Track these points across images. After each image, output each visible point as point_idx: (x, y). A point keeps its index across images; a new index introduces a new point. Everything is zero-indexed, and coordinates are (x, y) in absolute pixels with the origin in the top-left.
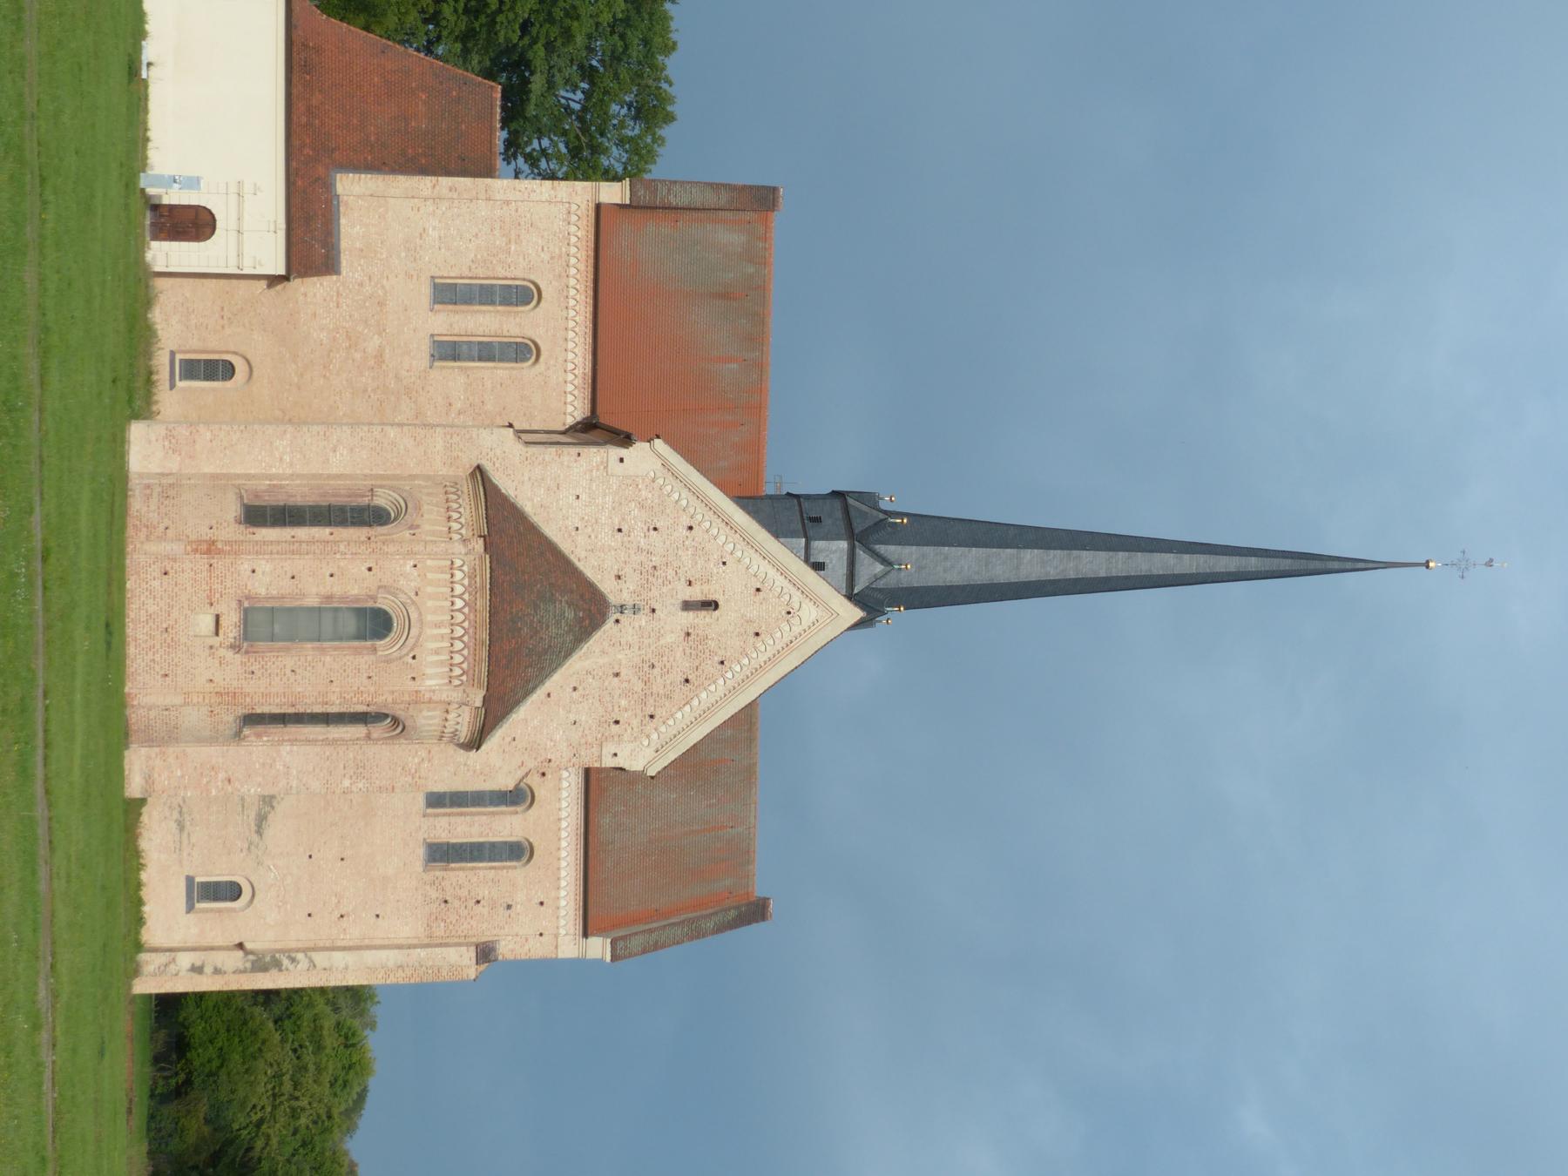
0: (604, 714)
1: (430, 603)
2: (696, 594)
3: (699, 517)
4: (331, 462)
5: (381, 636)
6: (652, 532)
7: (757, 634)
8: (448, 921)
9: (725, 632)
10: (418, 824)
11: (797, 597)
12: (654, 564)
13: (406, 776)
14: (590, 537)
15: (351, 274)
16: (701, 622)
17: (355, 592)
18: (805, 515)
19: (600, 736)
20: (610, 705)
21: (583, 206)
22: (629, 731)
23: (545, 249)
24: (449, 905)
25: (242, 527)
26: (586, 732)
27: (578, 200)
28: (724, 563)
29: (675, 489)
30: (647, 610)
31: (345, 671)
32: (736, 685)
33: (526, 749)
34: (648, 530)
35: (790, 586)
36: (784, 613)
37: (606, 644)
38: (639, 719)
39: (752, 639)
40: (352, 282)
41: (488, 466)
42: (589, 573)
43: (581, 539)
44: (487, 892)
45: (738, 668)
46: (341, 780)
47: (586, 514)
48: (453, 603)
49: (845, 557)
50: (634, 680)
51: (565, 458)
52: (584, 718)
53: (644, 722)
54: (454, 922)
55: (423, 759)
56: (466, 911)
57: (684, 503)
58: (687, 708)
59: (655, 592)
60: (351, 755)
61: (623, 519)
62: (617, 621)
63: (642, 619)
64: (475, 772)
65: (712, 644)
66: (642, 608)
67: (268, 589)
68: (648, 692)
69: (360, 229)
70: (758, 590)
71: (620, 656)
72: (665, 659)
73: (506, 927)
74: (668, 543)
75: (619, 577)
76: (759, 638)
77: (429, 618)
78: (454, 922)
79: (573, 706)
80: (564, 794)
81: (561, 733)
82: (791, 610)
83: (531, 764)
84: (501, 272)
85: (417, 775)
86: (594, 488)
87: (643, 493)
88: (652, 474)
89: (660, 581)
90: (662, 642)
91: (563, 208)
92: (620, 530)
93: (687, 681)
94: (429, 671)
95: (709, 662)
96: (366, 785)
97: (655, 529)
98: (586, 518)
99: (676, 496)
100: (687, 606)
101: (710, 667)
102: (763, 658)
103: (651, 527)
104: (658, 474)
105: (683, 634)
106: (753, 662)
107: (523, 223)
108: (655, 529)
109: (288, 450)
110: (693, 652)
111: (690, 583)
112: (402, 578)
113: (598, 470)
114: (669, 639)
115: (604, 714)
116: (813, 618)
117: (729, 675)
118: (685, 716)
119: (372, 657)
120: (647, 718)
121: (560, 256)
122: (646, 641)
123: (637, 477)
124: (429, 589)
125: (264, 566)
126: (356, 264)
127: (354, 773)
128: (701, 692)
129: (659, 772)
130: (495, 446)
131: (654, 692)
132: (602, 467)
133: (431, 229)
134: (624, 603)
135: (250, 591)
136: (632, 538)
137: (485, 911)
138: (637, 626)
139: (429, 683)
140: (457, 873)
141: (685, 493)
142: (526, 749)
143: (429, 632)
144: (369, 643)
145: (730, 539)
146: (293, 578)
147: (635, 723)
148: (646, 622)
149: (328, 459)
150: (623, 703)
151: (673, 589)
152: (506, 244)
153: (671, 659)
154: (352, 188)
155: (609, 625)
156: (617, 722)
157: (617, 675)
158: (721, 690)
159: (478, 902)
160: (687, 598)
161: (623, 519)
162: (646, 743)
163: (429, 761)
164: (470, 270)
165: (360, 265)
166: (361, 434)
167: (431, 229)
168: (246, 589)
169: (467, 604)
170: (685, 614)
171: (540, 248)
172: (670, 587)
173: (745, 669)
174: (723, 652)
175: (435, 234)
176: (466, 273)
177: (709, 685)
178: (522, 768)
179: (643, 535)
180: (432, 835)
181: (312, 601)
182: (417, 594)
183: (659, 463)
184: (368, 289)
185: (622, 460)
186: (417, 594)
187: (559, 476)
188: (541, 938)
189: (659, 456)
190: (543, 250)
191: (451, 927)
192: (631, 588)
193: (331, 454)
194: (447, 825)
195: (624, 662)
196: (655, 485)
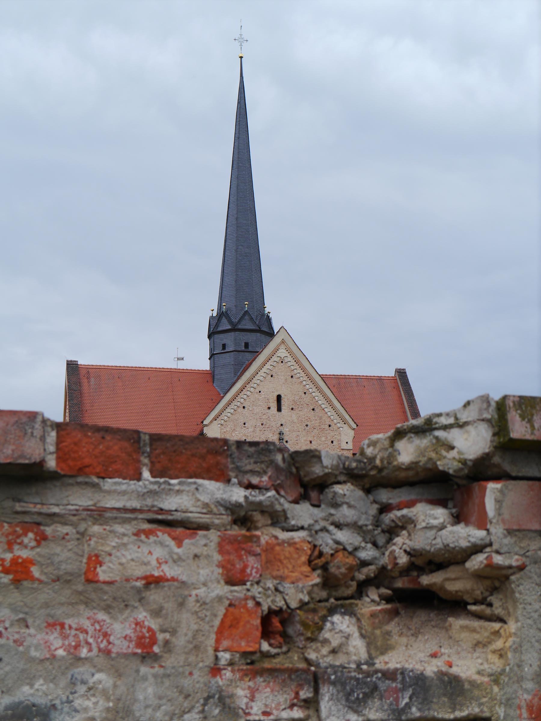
0: (329, 448)
3: (239, 403)
6: (246, 425)
7: (292, 377)
11: (275, 358)
12: (261, 424)
16: (287, 403)
18: (223, 351)
19: (338, 450)
20: (324, 445)
22: (336, 436)
28: (260, 392)
29: (226, 415)
30: (281, 428)
32: (315, 387)
34: (245, 427)
35: (270, 361)
36: (282, 364)
38: (330, 432)
45: (307, 386)
49: (242, 333)
50: (313, 434)
53: (332, 430)
57: (232, 411)
58: (326, 409)
62: (287, 442)
63: (285, 430)
65: (297, 397)
66: (280, 430)
68: (318, 428)
70: (272, 376)
71: (302, 441)
72: (303, 420)
74: (250, 418)
76: (294, 376)
82: (281, 361)
87: (228, 429)
90: (296, 421)
93: (313, 409)
95: (305, 399)
99: (229, 414)
100: (279, 409)
101: (307, 399)
102: (303, 374)
103: (244, 426)
105: (292, 411)
106: (305, 379)
108: (245, 424)
110: (300, 406)
111: (269, 408)
114: (295, 418)
115: (329, 448)
116: (285, 351)
117: (310, 390)
118: (329, 411)
120: (330, 428)
122: (296, 428)
123: (221, 432)
129: (355, 423)
131: (318, 425)
134: (278, 438)
136: (249, 435)
138: (288, 433)
141: (228, 410)
145: (249, 389)
151: (272, 416)
153: (303, 417)
155: (288, 445)
156: (332, 442)
157: (311, 442)
158: (317, 394)
160: (276, 409)
162: (341, 429)
170: (283, 410)
172: (271, 417)
173: (308, 383)
174: (300, 392)
177: (315, 399)
179: (247, 430)
189: (211, 422)
192: (271, 435)
195: (305, 439)
196: (224, 424)
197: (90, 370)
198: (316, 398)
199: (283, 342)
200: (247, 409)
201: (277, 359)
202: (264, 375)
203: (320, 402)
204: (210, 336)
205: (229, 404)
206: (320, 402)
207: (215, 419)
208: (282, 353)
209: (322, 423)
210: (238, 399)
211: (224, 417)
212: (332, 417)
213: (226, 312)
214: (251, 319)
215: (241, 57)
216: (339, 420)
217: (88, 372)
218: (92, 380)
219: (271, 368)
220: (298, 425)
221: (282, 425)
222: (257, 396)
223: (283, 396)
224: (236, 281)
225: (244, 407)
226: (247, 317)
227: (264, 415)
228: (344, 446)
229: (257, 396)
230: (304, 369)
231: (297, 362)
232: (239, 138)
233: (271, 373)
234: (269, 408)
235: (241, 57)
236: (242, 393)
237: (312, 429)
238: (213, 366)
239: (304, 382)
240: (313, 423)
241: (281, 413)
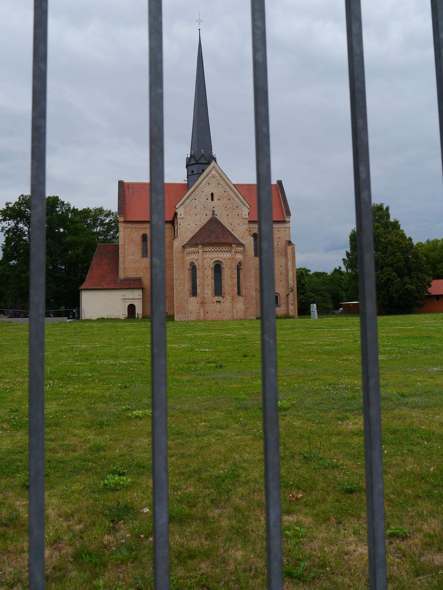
1: (213, 256)
2: (210, 198)
3: (193, 197)
5: (220, 266)
7: (218, 184)
11: (210, 175)
17: (211, 272)
21: (124, 225)
25: (197, 296)
27: (123, 226)
30: (213, 209)
39: (219, 185)
41: (183, 244)
42: (206, 222)
43: (198, 223)
48: (213, 251)
50: (229, 211)
51: (180, 227)
57: (190, 201)
59: (210, 207)
62: (216, 215)
63: (215, 209)
70: (209, 184)
75: (206, 215)
77: (216, 256)
83: (248, 233)
84: (140, 243)
90: (220, 205)
91: (125, 229)
93: (229, 199)
94: (228, 256)
100: (212, 200)
101: (226, 194)
114: (220, 204)
116: (215, 172)
117: (228, 190)
119: (225, 268)
124: (210, 256)
125: (206, 292)
137: (280, 243)
139: (230, 256)
141: (187, 201)
143: (219, 256)
144: (222, 269)
147: (239, 211)
154: (122, 275)
155: (217, 217)
156: (238, 215)
157: (228, 215)
158: (231, 192)
161: (194, 214)
169: (213, 248)
176: (140, 250)
181: (213, 281)
183: (181, 207)
184: (145, 271)
185: (181, 215)
189: (179, 206)
196: (186, 207)
197: (129, 184)
198: (230, 194)
199: (214, 167)
201: (211, 176)
202: (205, 183)
203: (232, 196)
204: (187, 166)
205: (188, 198)
206: (232, 196)
207: (181, 205)
208: (214, 172)
211: (186, 204)
212: (238, 203)
213: (193, 155)
214: (205, 158)
215: (199, 29)
216: (242, 204)
217: (129, 186)
218: (130, 190)
219: (208, 180)
221: (214, 207)
223: (214, 193)
224: (198, 140)
225: (195, 199)
226: (203, 157)
228: (244, 217)
230: (224, 181)
231: (221, 177)
232: (199, 70)
234: (207, 199)
235: (199, 29)
236: (194, 192)
238: (188, 181)
239: (224, 187)
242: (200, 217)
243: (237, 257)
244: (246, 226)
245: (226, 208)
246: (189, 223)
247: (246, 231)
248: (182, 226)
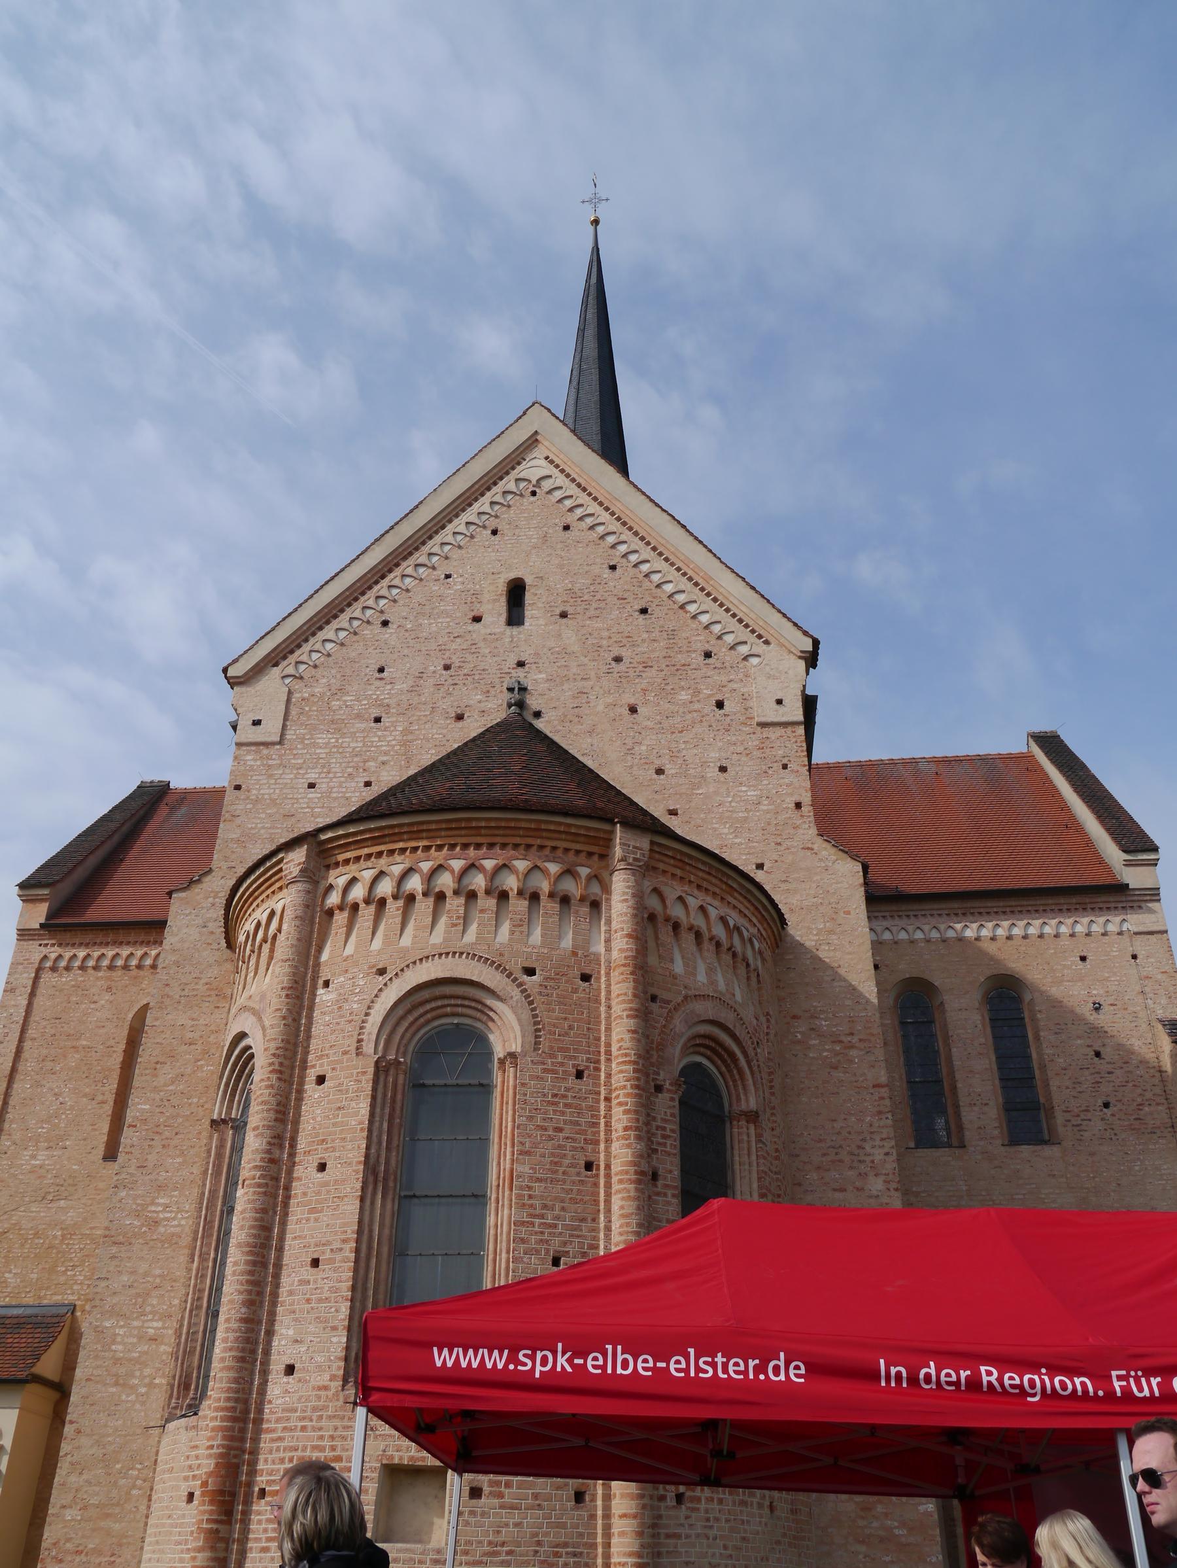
0: (705, 724)
2: (495, 610)
4: (178, 1230)
8: (1139, 1100)
9: (561, 566)
10: (979, 1157)
11: (508, 483)
12: (440, 667)
13: (851, 1061)
14: (383, 763)
15: (75, 1287)
20: (689, 716)
22: (735, 686)
23: (95, 998)
24: (1112, 1100)
26: (740, 749)
30: (520, 672)
31: (560, 1130)
33: (779, 844)
36: (532, 499)
37: (576, 729)
40: (89, 1286)
44: (1079, 1042)
46: (870, 1197)
47: (343, 772)
51: (239, 807)
52: (714, 755)
53: (719, 665)
54: (1139, 1091)
55: (812, 1029)
56: (1118, 1072)
60: (815, 1176)
61: (358, 716)
63: (534, 679)
64: (831, 932)
67: (334, 1328)
69: (10, 1272)
70: (494, 532)
71: (600, 708)
72: (605, 643)
73: (1131, 1009)
74: (406, 652)
78: (1139, 1091)
79: (692, 771)
80: (903, 935)
81: (744, 789)
85: (846, 1039)
86: (300, 761)
88: (287, 681)
89: (469, 658)
92: (378, 720)
93: (644, 611)
94: (567, 942)
96: (877, 1143)
97: (381, 670)
98: (350, 770)
101: (618, 582)
103: (378, 675)
104: (290, 670)
107: (53, 1031)
108: (381, 670)
109: (136, 1323)
110: (594, 605)
112: (346, 1006)
113: (269, 758)
116: (544, 463)
121: (109, 979)
126: (62, 1279)
127: (851, 1168)
128: (664, 592)
129: (806, 633)
130: (199, 921)
131: (664, 654)
132: (265, 751)
133: (33, 1162)
135: (333, 1378)
136: (392, 702)
140: (1054, 1089)
141: (328, 632)
142: (779, 844)
146: (315, 1263)
148: (540, 672)
149: (173, 1235)
150: (684, 696)
152: (78, 1051)
156: (720, 705)
157: (633, 710)
159: (1098, 1054)
161: (358, 716)
162: (754, 661)
163: (813, 1017)
164: (103, 1102)
165: (65, 1272)
166: (132, 1170)
167: (33, 1162)
168: (326, 1388)
171: (93, 1006)
172: (481, 644)
175: (42, 1156)
178: (815, 847)
179: (389, 687)
180: (996, 1132)
182: (382, 972)
186: (382, 972)
187: (270, 816)
188: (1140, 957)
190: (95, 1002)
191: (1148, 1095)
192: (479, 697)
193: (162, 1230)
194: (976, 1109)
195: (610, 700)
200: (395, 626)
209: (677, 649)
210: (369, 599)
220: (586, 660)
222: (437, 588)
223: (528, 581)
227: (458, 640)
229: (437, 588)
233: (492, 523)
235: (596, 222)
237: (637, 670)
240: (643, 648)
241: (521, 628)
242: (406, 732)
243: (678, 967)
244: (788, 777)
245: (622, 667)
246: (312, 776)
247: (792, 813)
248: (257, 801)
